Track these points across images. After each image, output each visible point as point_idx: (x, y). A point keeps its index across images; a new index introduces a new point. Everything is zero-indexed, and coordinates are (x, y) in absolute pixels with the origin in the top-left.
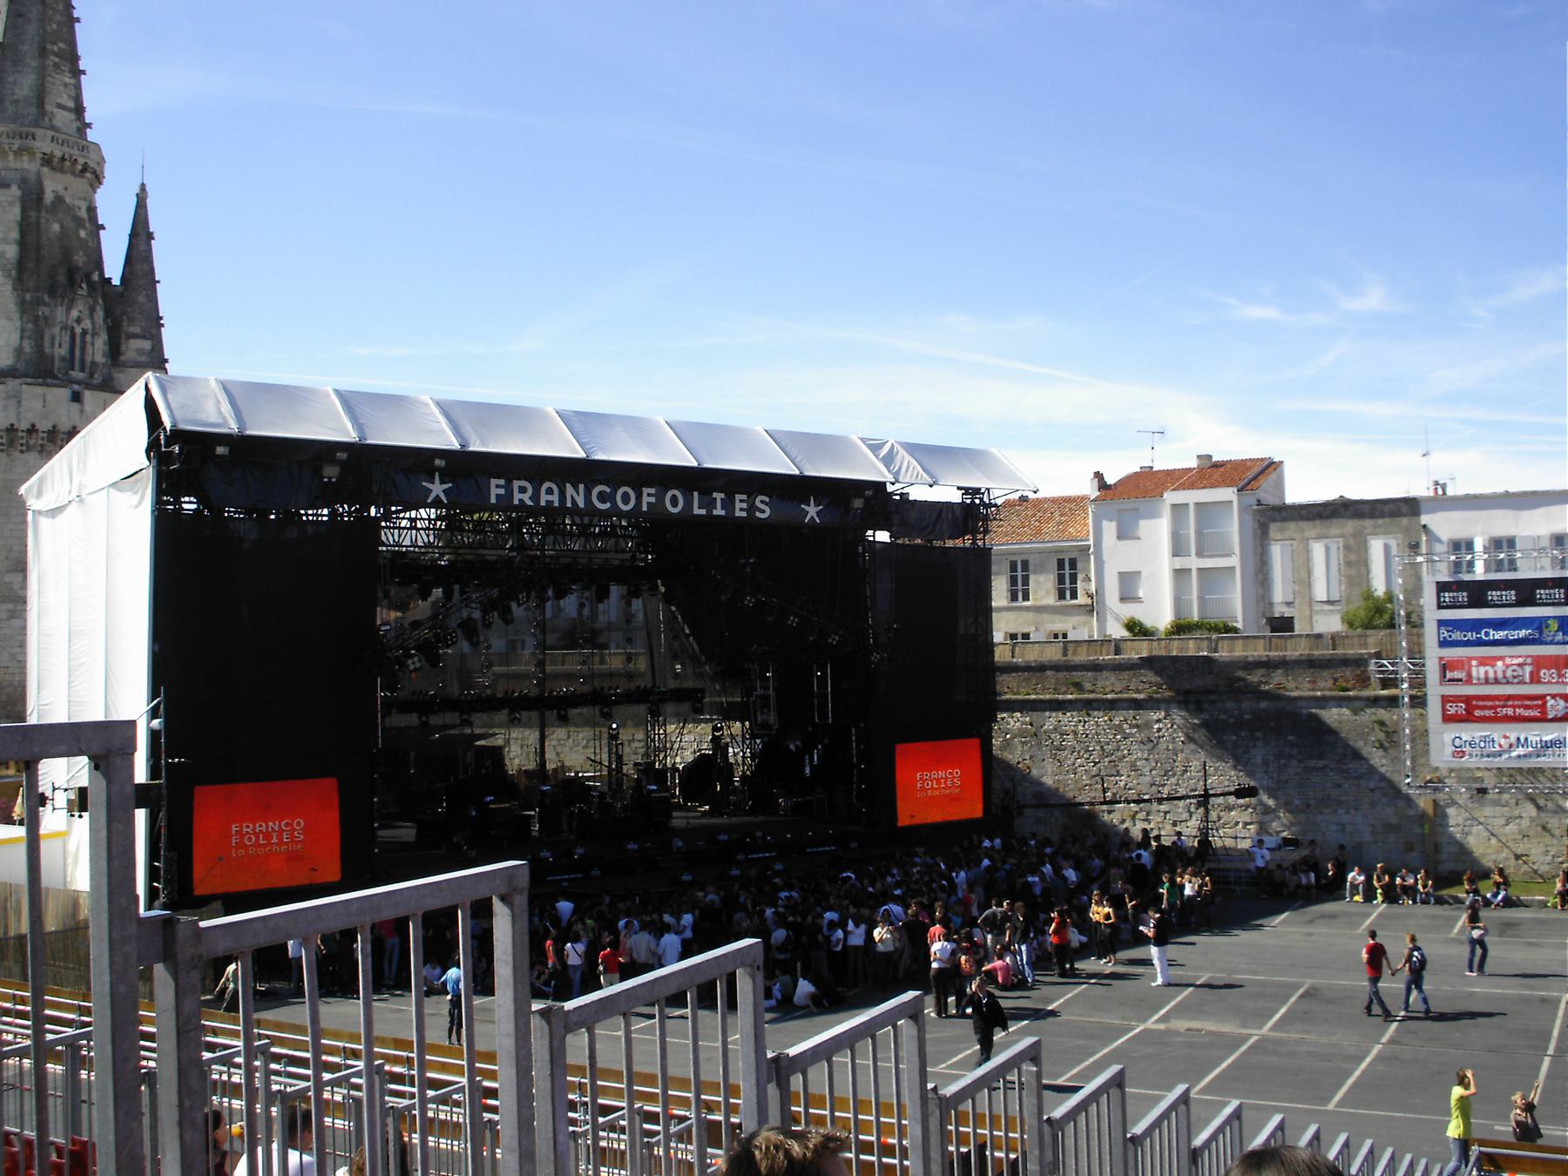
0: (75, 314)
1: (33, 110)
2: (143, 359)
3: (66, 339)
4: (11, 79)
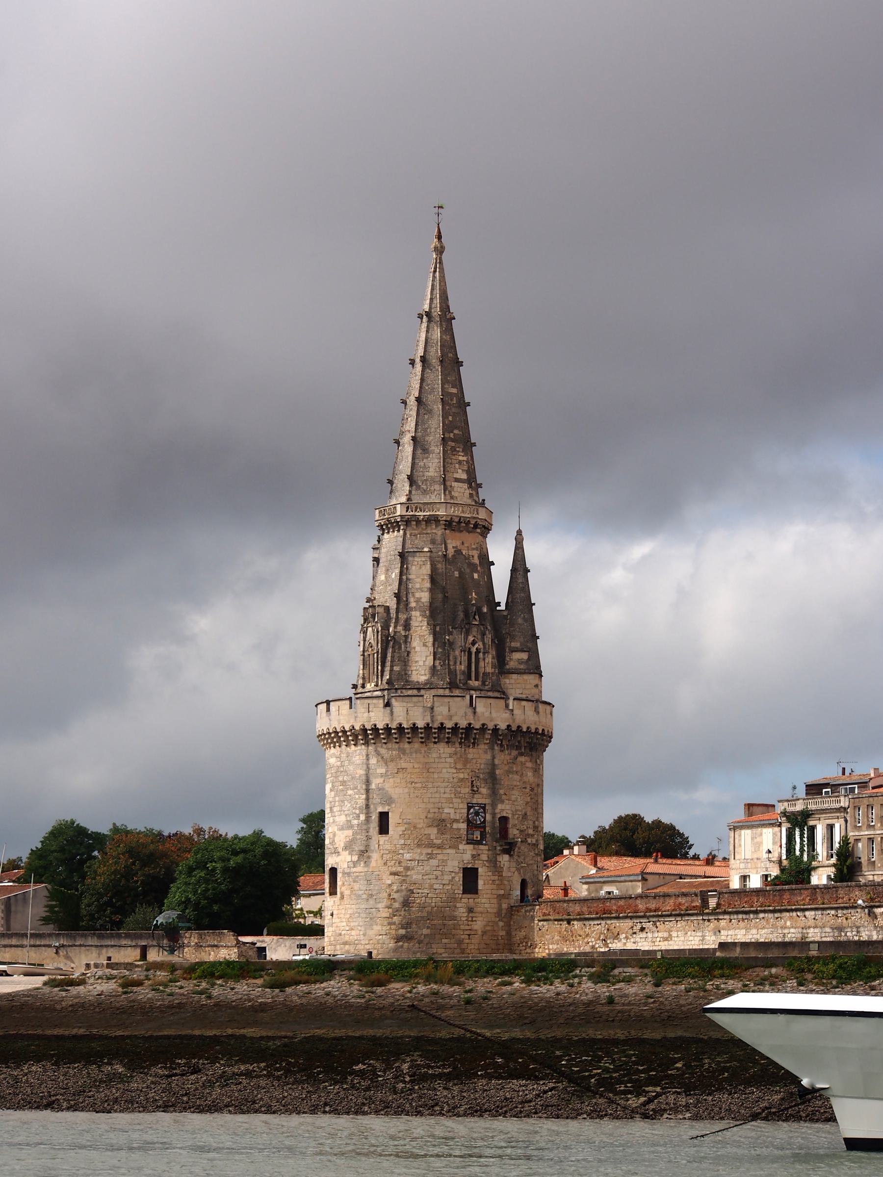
0: (471, 639)
1: (439, 488)
2: (522, 667)
3: (465, 658)
4: (421, 464)
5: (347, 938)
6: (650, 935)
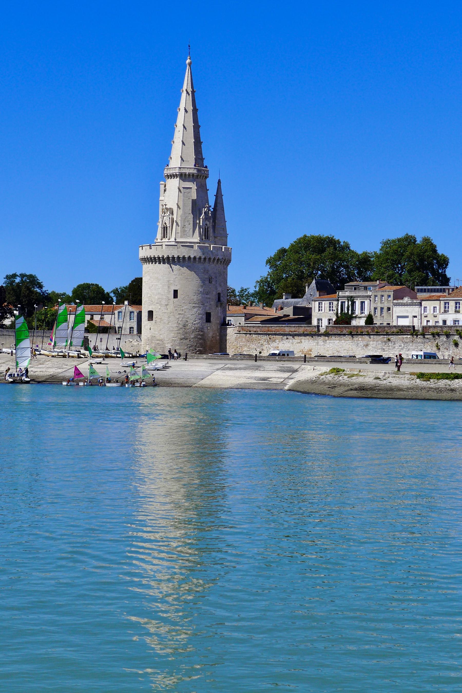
5: (158, 338)
6: (291, 341)
